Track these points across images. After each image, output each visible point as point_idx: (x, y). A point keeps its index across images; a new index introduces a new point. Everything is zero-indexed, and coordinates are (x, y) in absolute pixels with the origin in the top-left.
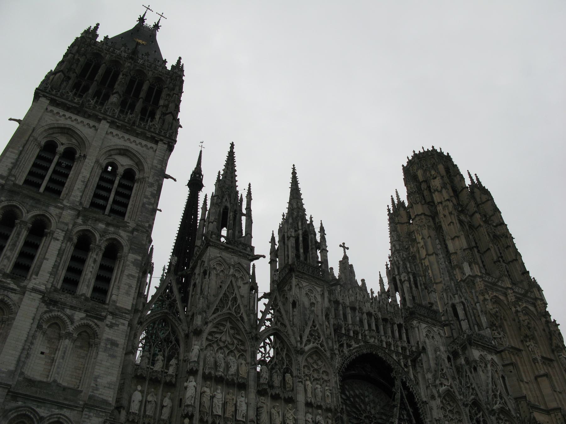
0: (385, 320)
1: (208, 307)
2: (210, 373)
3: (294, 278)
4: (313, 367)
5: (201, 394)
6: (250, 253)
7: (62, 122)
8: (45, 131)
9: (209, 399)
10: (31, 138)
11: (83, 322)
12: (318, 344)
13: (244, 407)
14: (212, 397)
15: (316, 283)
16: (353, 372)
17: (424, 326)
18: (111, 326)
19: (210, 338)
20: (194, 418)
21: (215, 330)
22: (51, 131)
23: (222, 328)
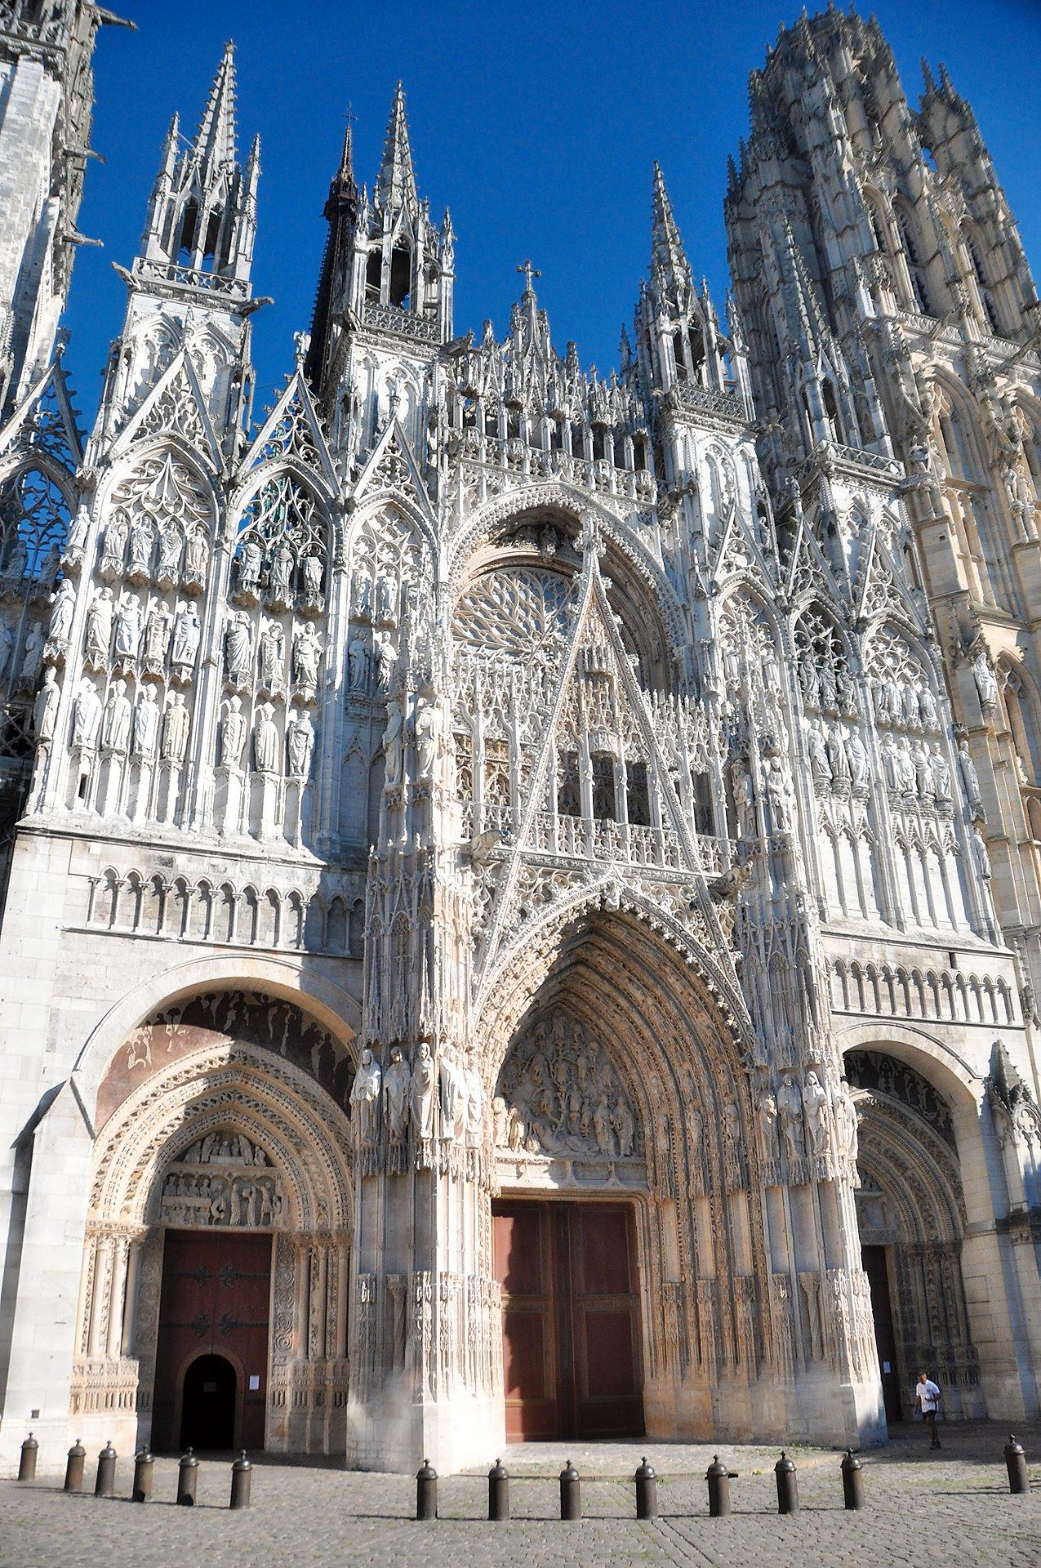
0: (600, 430)
1: (120, 428)
3: (353, 347)
4: (380, 539)
5: (89, 615)
9: (108, 622)
13: (193, 634)
15: (414, 354)
17: (700, 434)
19: (121, 494)
20: (68, 666)
21: (136, 476)
23: (152, 471)
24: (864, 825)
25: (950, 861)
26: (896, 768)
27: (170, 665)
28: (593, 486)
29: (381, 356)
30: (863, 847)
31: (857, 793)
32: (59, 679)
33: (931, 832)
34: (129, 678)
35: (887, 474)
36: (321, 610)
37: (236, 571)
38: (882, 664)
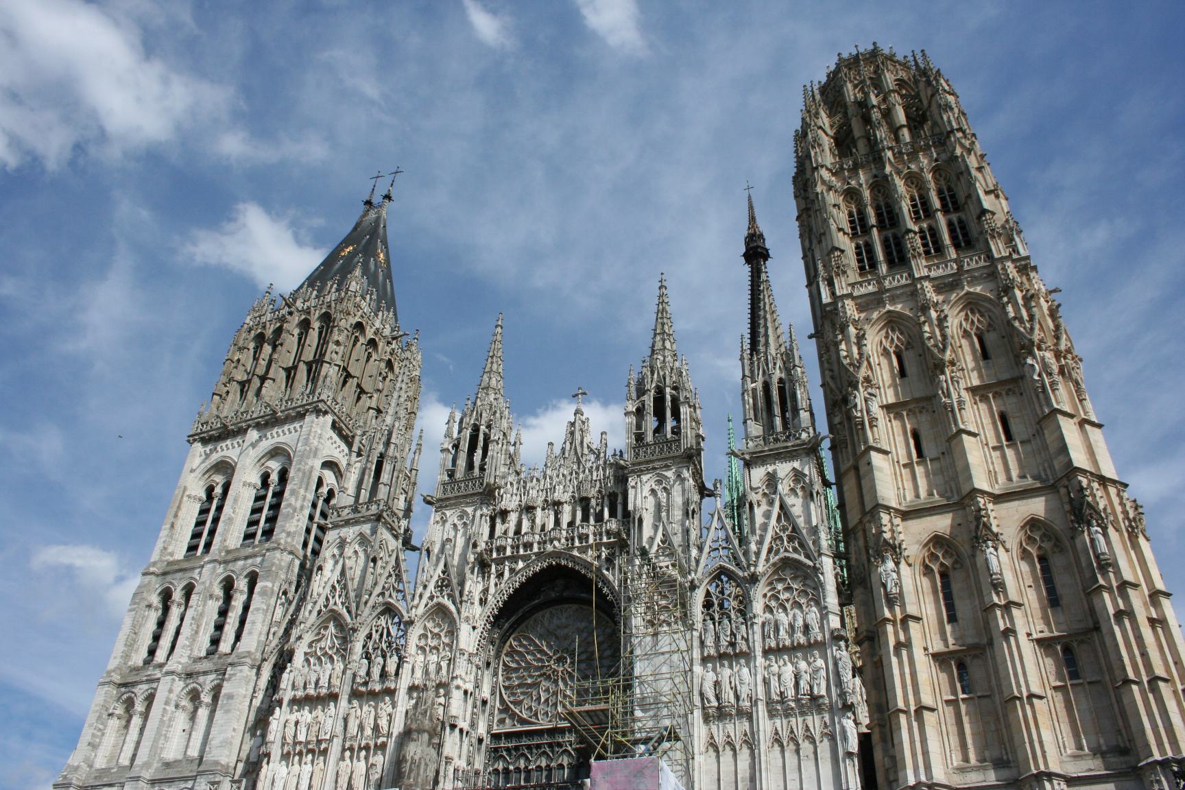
1: (310, 611)
2: (295, 696)
4: (431, 632)
6: (375, 512)
7: (215, 457)
8: (200, 479)
9: (293, 723)
10: (185, 499)
11: (213, 684)
12: (443, 597)
13: (330, 721)
14: (297, 723)
16: (536, 601)
17: (645, 478)
18: (229, 680)
19: (309, 651)
22: (206, 476)
24: (746, 735)
25: (824, 747)
26: (774, 683)
27: (319, 742)
28: (577, 543)
29: (448, 513)
30: (744, 754)
31: (741, 713)
32: (268, 763)
33: (807, 726)
34: (300, 754)
35: (798, 442)
36: (393, 688)
37: (354, 675)
38: (778, 599)
